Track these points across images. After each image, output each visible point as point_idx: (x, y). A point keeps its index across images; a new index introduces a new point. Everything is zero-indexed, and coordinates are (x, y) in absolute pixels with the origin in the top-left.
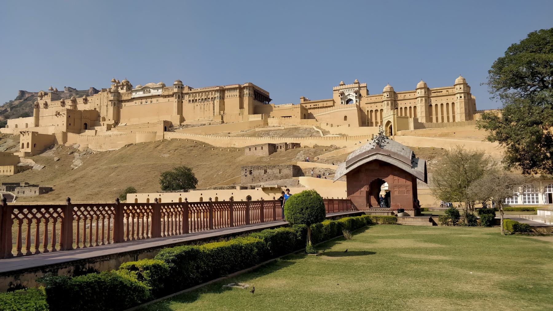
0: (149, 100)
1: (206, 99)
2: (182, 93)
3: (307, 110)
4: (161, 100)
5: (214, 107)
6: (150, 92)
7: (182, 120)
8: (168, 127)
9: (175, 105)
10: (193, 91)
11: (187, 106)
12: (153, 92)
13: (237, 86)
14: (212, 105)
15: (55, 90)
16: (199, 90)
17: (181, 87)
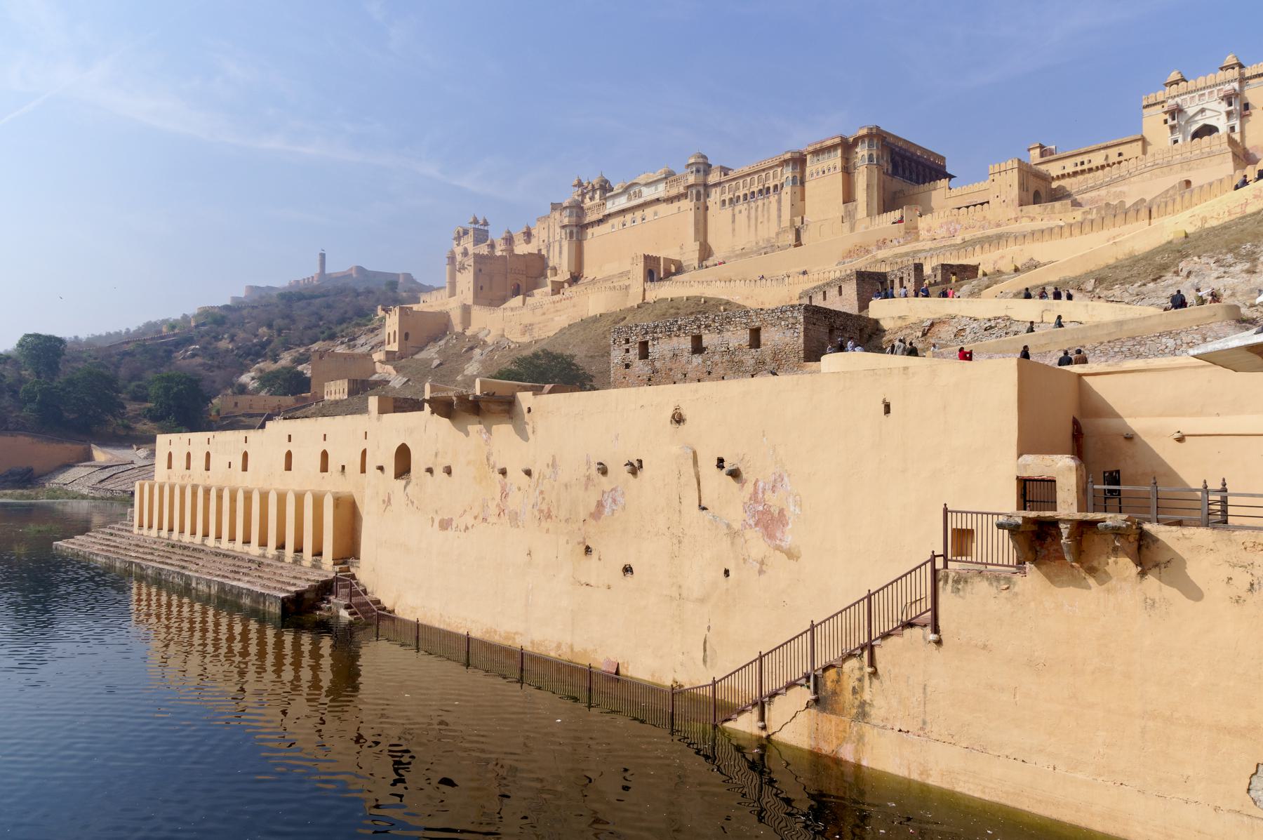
0: (639, 214)
1: (760, 191)
2: (706, 186)
3: (1046, 179)
4: (663, 208)
5: (779, 210)
6: (640, 194)
7: (705, 252)
8: (654, 271)
9: (691, 217)
10: (731, 175)
11: (718, 217)
12: (649, 194)
13: (838, 140)
14: (774, 206)
15: (481, 222)
16: (746, 170)
17: (704, 167)
